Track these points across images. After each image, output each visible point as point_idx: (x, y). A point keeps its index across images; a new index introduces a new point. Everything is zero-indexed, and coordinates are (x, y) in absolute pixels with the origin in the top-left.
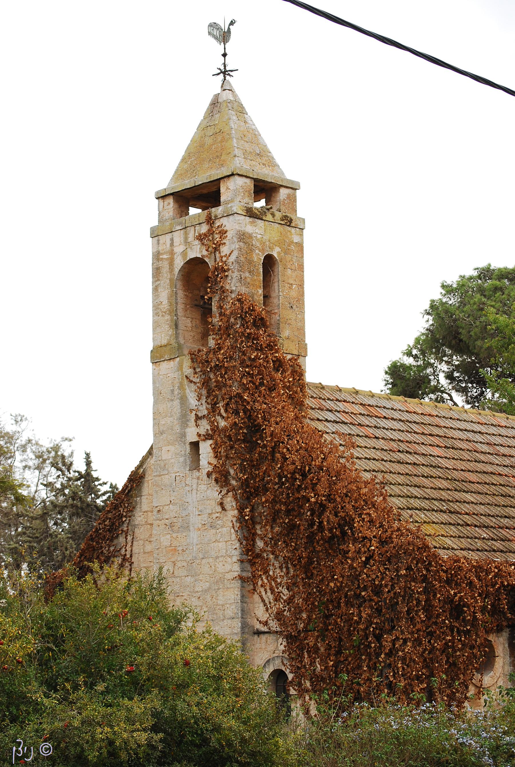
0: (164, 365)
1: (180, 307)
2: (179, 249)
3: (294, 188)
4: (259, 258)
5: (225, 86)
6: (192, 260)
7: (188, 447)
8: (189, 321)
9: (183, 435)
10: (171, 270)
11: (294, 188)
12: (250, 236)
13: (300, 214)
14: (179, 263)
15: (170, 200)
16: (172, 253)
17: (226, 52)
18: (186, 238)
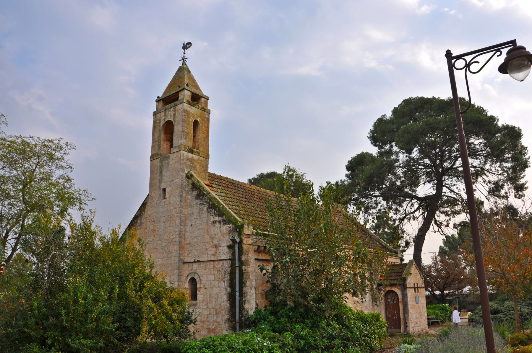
0: (155, 161)
1: (162, 139)
2: (162, 118)
3: (207, 99)
4: (192, 120)
5: (184, 63)
6: (167, 121)
7: (162, 191)
8: (165, 145)
9: (160, 187)
10: (159, 126)
11: (207, 99)
12: (189, 112)
13: (209, 108)
14: (162, 123)
15: (161, 102)
16: (160, 119)
17: (188, 63)
18: (165, 114)
